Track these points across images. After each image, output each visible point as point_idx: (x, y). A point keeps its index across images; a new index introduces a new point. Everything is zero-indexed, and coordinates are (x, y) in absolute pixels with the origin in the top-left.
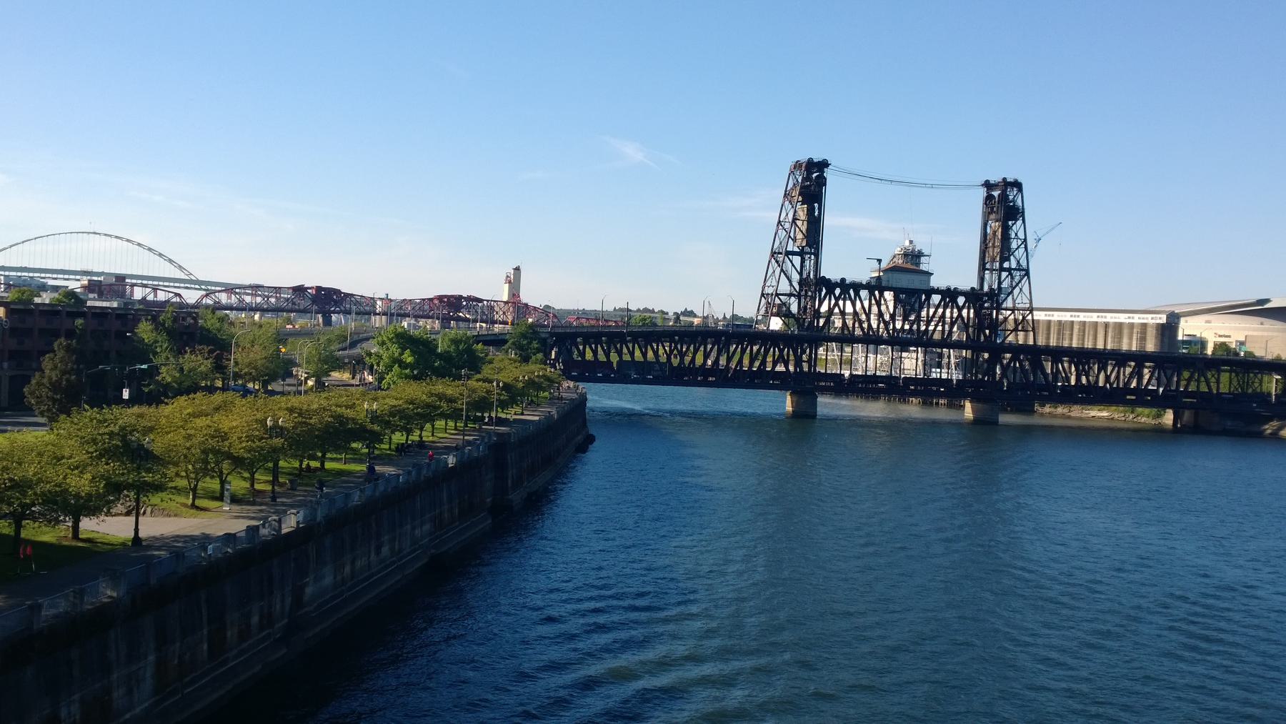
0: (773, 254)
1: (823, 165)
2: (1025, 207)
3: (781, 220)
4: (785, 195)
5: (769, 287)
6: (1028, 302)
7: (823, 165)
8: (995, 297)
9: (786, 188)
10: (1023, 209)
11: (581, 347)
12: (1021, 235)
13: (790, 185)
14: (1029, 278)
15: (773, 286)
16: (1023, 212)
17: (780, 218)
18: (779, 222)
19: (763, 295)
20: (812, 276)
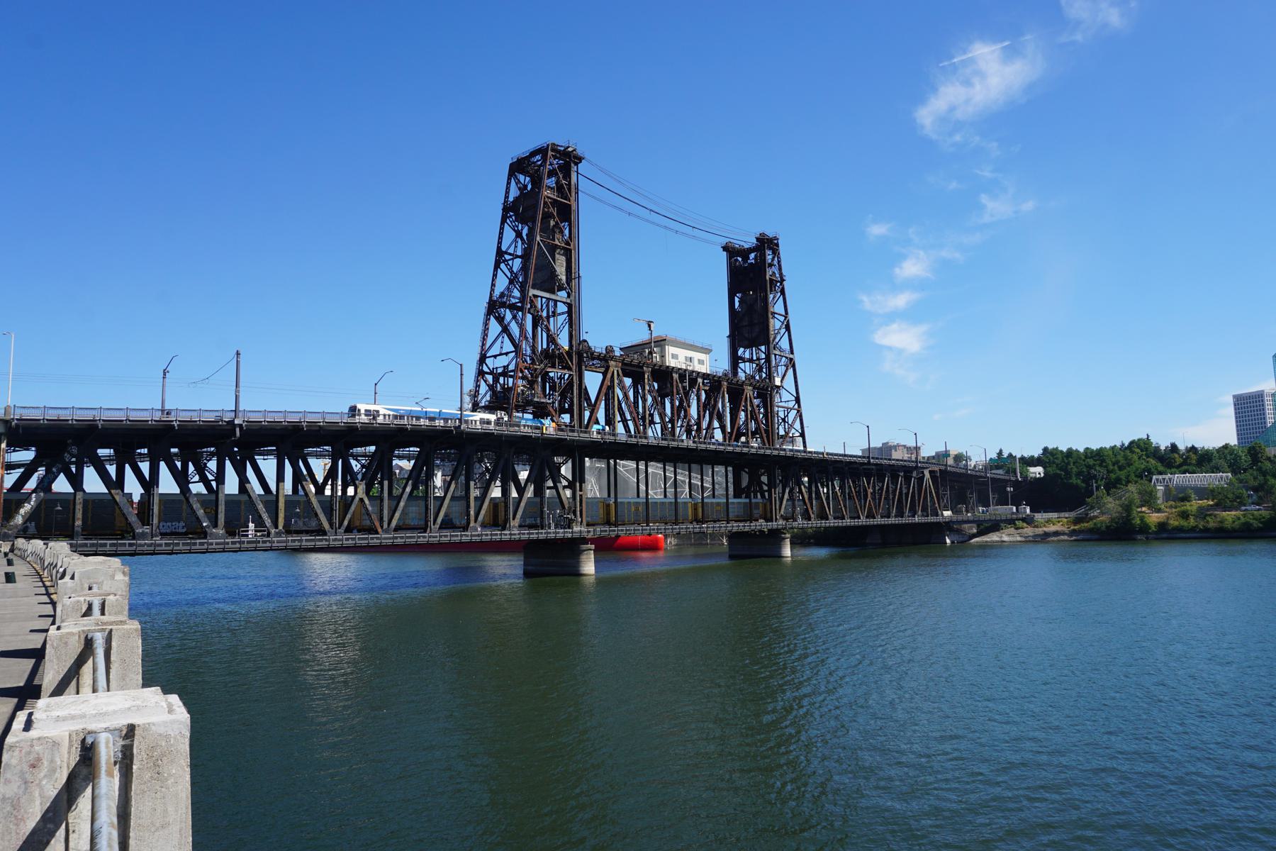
0: (494, 307)
1: (568, 159)
2: (784, 272)
3: (504, 248)
4: (507, 209)
5: (495, 356)
6: (794, 399)
7: (568, 159)
8: (766, 392)
9: (507, 197)
10: (781, 274)
11: (112, 470)
12: (779, 308)
13: (514, 192)
14: (794, 366)
15: (507, 354)
16: (782, 280)
17: (500, 243)
18: (500, 253)
19: (481, 373)
20: (563, 342)
